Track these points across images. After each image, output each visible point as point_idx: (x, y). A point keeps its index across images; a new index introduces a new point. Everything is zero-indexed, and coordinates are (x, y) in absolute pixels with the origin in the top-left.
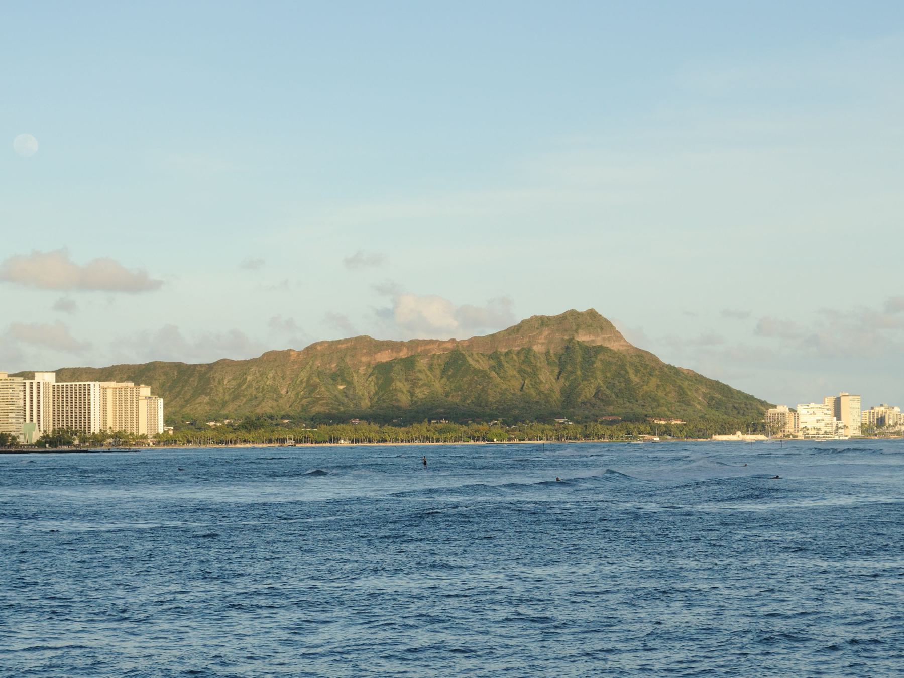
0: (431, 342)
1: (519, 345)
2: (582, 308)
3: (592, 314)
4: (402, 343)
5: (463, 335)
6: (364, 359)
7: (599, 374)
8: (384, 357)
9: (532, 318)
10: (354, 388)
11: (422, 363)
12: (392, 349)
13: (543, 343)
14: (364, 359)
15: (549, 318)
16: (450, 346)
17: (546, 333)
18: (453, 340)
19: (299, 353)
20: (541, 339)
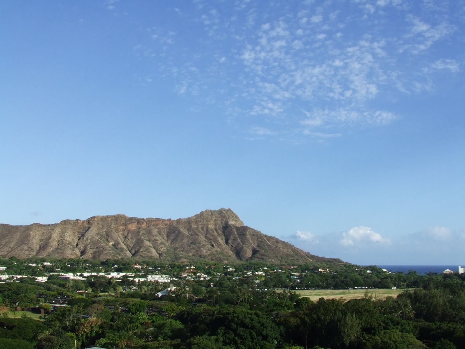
0: (159, 220)
1: (202, 225)
2: (227, 208)
3: (230, 210)
4: (143, 219)
5: (174, 218)
6: (121, 227)
7: (250, 241)
8: (133, 227)
9: (206, 211)
10: (119, 243)
11: (155, 231)
12: (138, 223)
13: (213, 224)
14: (121, 227)
15: (214, 211)
16: (168, 222)
17: (214, 219)
18: (170, 220)
19: (83, 222)
20: (212, 222)
